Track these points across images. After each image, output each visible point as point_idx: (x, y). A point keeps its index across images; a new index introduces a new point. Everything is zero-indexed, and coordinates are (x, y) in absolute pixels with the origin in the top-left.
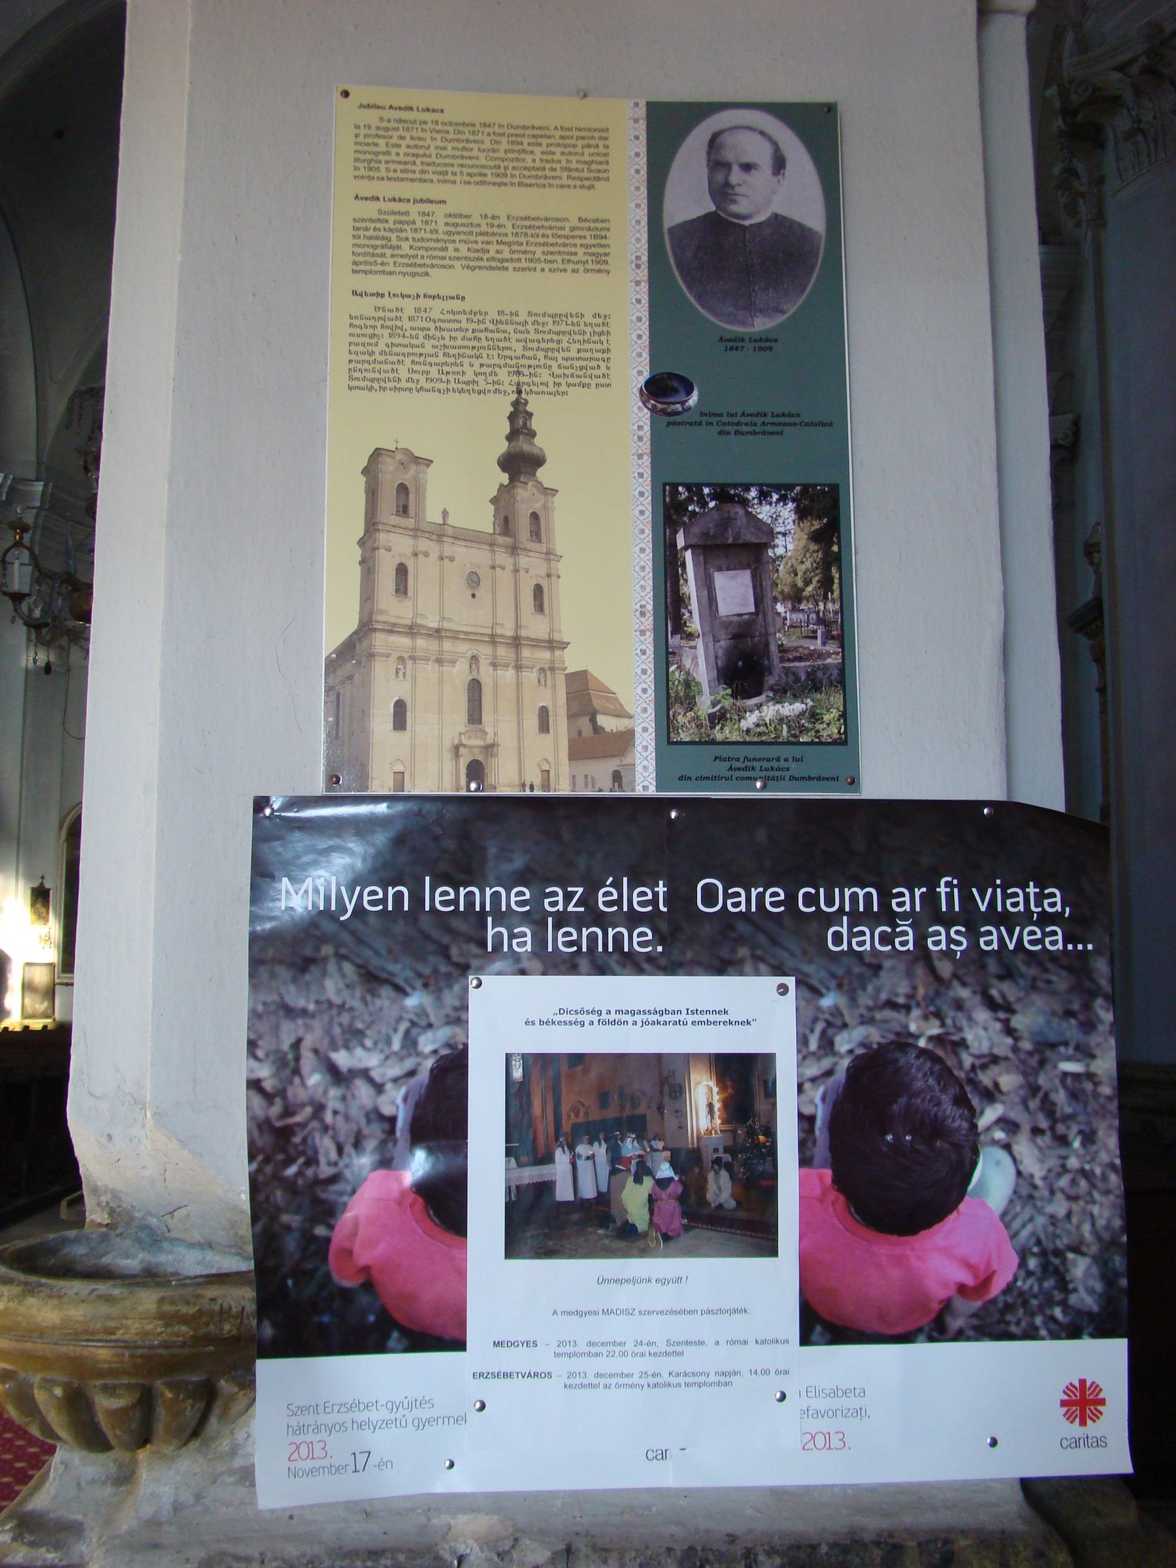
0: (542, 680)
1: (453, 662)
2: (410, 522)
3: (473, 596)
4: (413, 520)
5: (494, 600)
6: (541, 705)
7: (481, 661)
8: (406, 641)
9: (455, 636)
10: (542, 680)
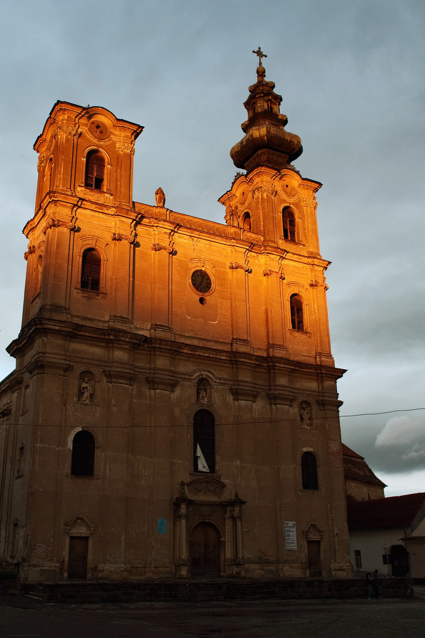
1: (172, 386)
6: (305, 450)
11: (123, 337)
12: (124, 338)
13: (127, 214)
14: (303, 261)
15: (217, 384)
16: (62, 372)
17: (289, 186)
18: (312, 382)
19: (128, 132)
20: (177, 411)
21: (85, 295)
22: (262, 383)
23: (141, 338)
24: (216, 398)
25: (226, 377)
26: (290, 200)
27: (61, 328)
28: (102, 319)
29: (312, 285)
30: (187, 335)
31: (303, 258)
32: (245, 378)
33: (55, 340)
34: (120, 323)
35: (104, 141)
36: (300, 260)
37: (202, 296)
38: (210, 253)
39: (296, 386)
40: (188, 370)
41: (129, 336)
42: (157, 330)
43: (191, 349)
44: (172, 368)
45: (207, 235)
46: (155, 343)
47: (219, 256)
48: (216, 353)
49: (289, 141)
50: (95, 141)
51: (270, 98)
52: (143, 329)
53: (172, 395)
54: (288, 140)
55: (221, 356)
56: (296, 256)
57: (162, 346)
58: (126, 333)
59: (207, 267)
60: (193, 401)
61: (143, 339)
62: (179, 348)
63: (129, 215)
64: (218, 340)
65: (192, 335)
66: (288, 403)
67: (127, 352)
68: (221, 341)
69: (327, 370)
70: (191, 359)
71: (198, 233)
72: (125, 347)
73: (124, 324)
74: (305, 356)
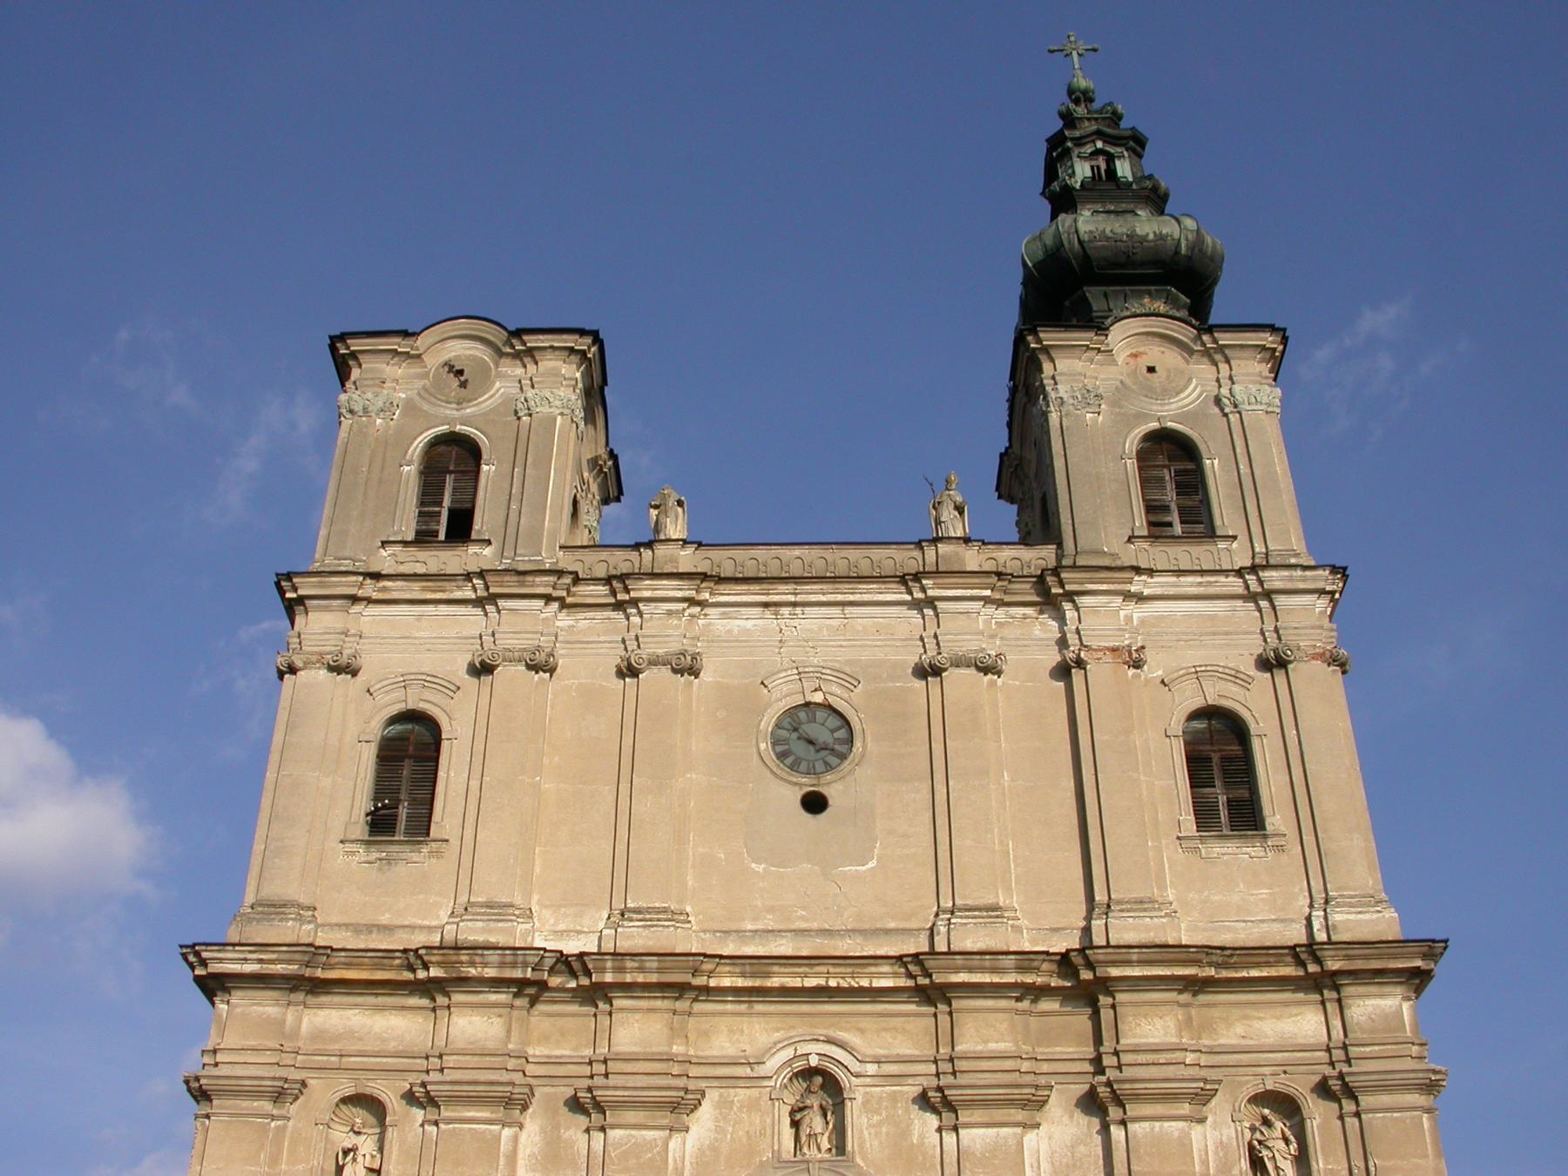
2: (476, 556)
3: (814, 803)
5: (940, 817)
7: (858, 1095)
11: (472, 964)
12: (479, 969)
13: (522, 584)
14: (1225, 590)
15: (868, 1080)
17: (1157, 369)
18: (1296, 1015)
19: (550, 360)
21: (375, 855)
22: (1070, 1050)
23: (537, 959)
24: (866, 1133)
25: (908, 1052)
26: (1166, 408)
27: (265, 966)
28: (426, 923)
29: (1264, 664)
30: (750, 927)
31: (1222, 579)
32: (986, 1042)
33: (255, 1007)
34: (480, 924)
35: (475, 402)
36: (1212, 590)
37: (813, 785)
38: (844, 643)
39: (1222, 1041)
40: (747, 1047)
41: (493, 956)
42: (623, 926)
43: (748, 968)
44: (676, 1049)
45: (824, 587)
46: (603, 970)
47: (879, 643)
48: (849, 970)
49: (1151, 236)
50: (450, 411)
51: (1099, 144)
52: (579, 932)
53: (675, 1142)
54: (1148, 234)
55: (871, 976)
56: (1190, 579)
57: (628, 975)
58: (480, 952)
59: (835, 689)
61: (549, 962)
62: (696, 972)
63: (529, 586)
64: (878, 926)
65: (769, 922)
66: (1185, 1108)
67: (500, 1016)
68: (892, 925)
69: (1348, 958)
70: (759, 1008)
71: (791, 587)
72: (493, 997)
73: (492, 924)
74: (1263, 921)
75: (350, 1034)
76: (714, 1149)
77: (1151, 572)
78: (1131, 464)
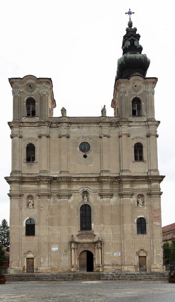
0: (141, 202)
1: (69, 196)
2: (37, 119)
4: (38, 118)
6: (139, 217)
8: (33, 187)
9: (69, 181)
10: (141, 202)
16: (19, 197)
20: (72, 207)
22: (116, 189)
44: (69, 189)
60: (80, 201)
75: (28, 188)
76: (74, 201)
77: (132, 122)
78: (131, 103)
